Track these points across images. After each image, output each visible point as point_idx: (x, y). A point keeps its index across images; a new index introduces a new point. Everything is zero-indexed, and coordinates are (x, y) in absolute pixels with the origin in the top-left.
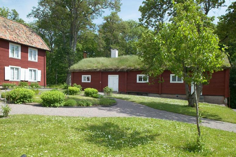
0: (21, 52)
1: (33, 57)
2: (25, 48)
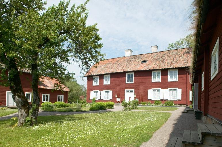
0: (161, 75)
1: (173, 78)
2: (165, 72)
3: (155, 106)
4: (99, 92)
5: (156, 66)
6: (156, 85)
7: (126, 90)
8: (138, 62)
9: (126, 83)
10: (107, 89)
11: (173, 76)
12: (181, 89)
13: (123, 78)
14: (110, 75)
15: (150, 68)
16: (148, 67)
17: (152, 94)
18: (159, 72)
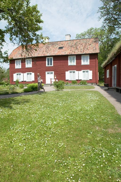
0: (76, 60)
1: (85, 62)
2: (79, 57)
3: (73, 85)
4: (22, 74)
5: (71, 52)
6: (72, 68)
7: (46, 72)
8: (55, 48)
9: (46, 66)
10: (29, 72)
11: (85, 61)
12: (92, 71)
13: (43, 62)
14: (31, 59)
15: (67, 53)
16: (65, 53)
17: (69, 76)
18: (74, 57)
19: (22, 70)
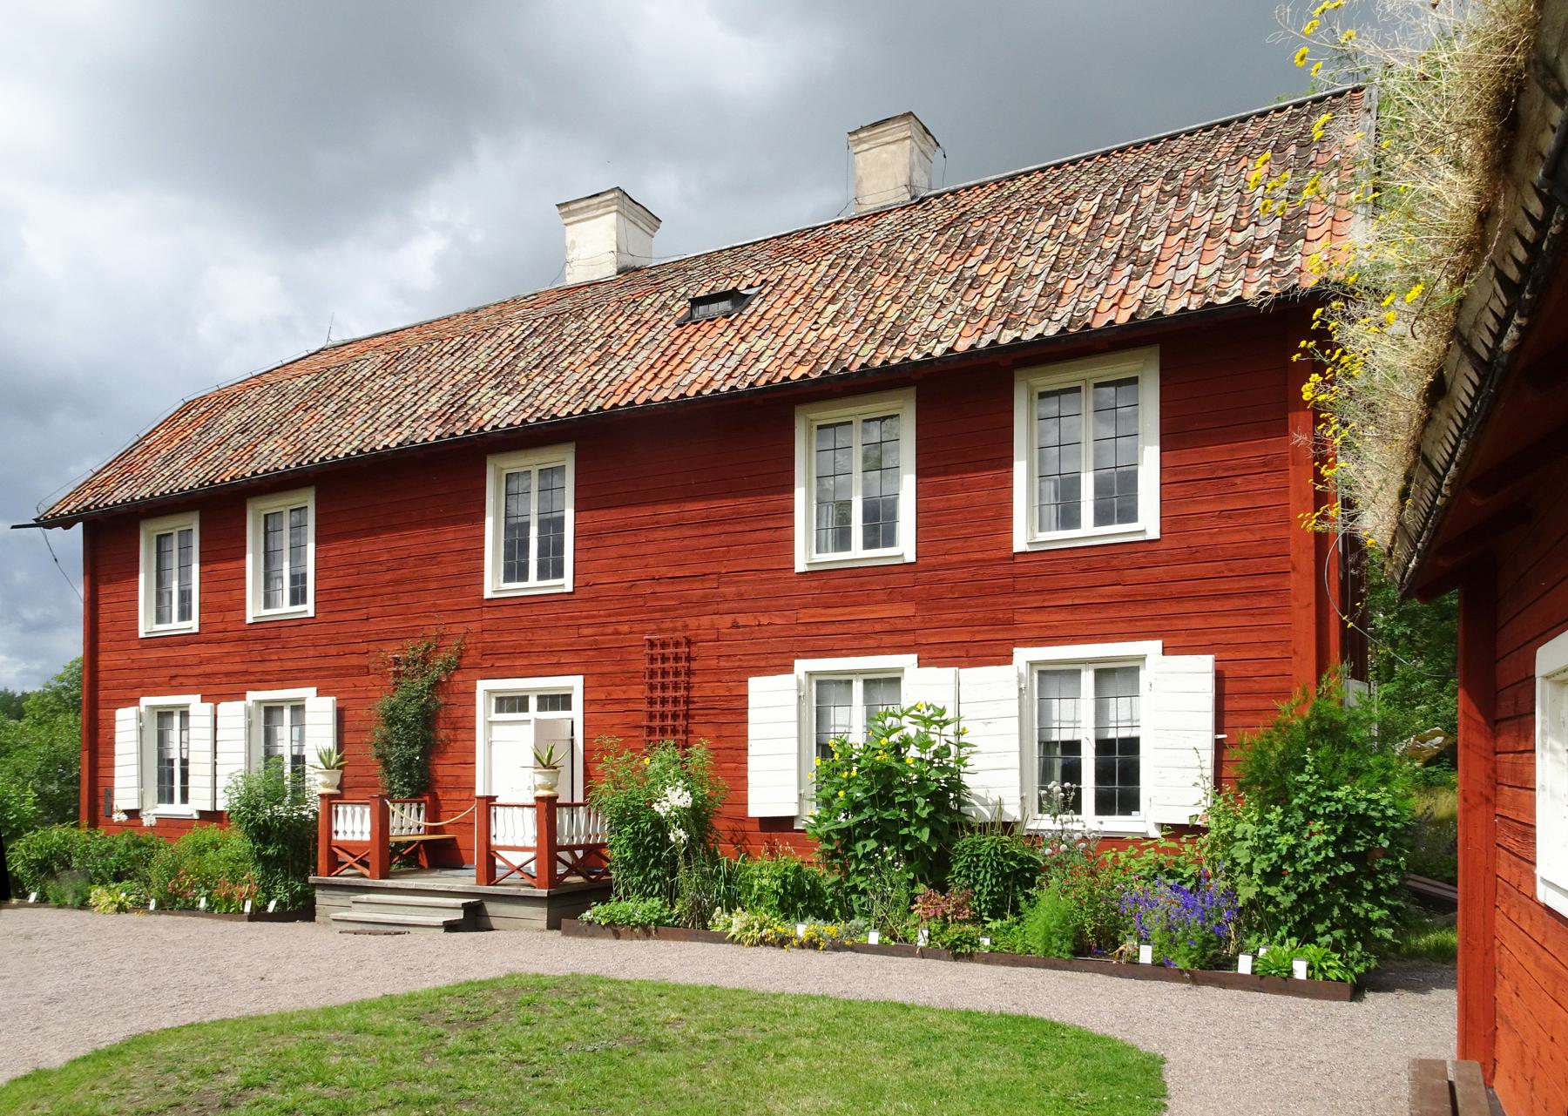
7: (482, 686)
12: (1206, 663)
19: (209, 661)
